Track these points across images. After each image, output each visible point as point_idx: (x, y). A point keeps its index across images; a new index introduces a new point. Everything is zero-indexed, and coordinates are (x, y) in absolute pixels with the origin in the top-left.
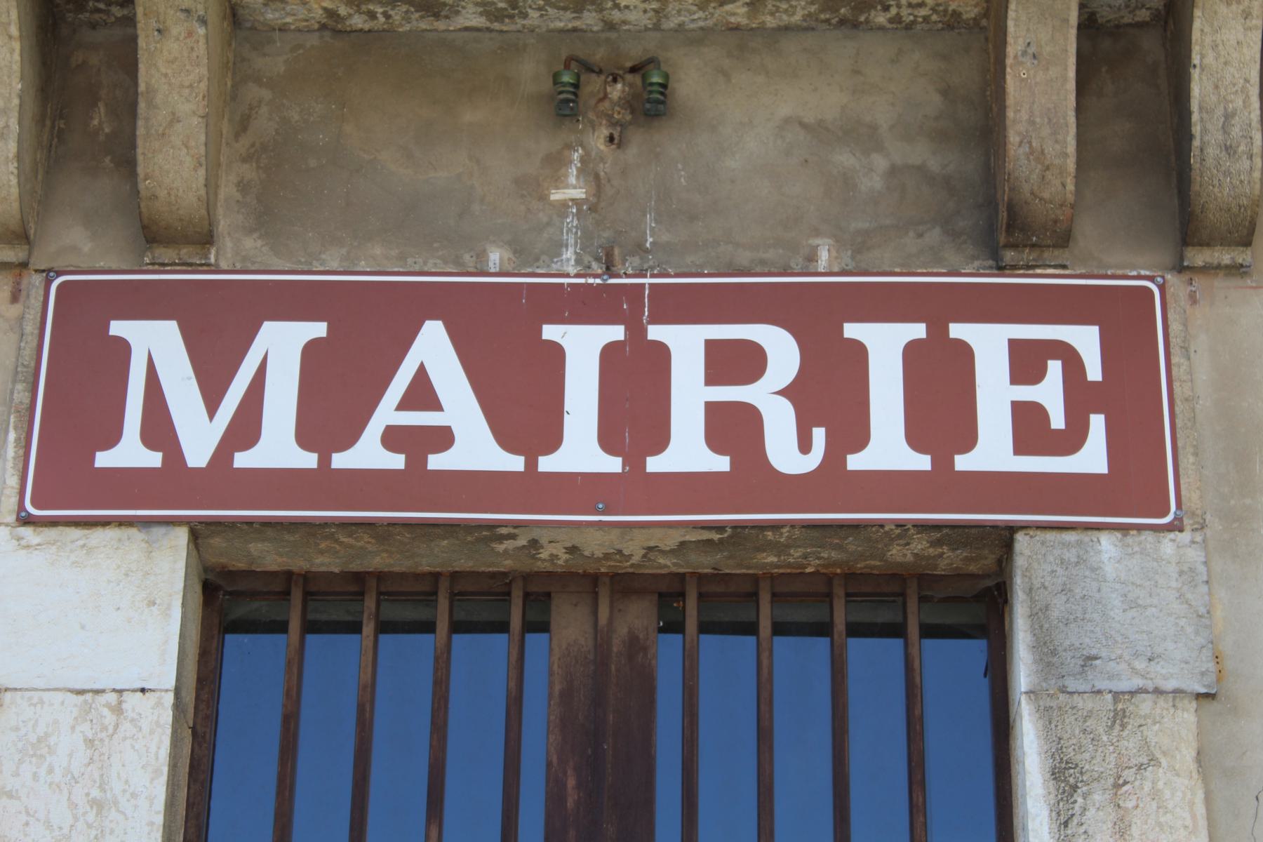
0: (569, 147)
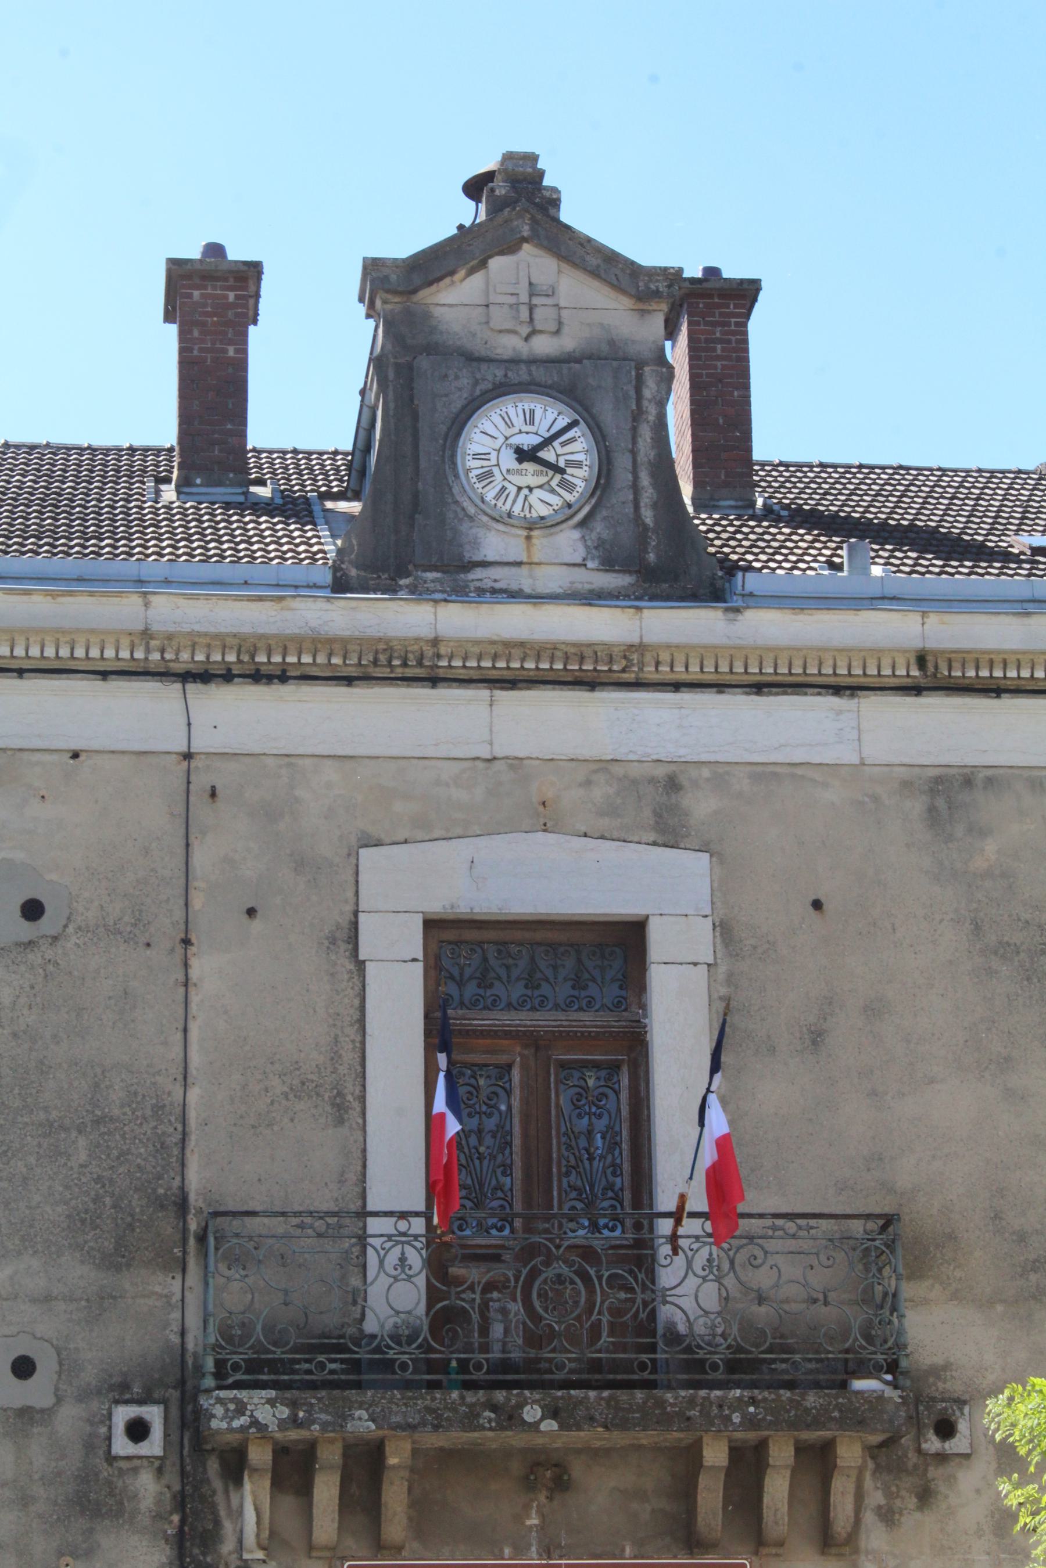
0: (532, 1500)
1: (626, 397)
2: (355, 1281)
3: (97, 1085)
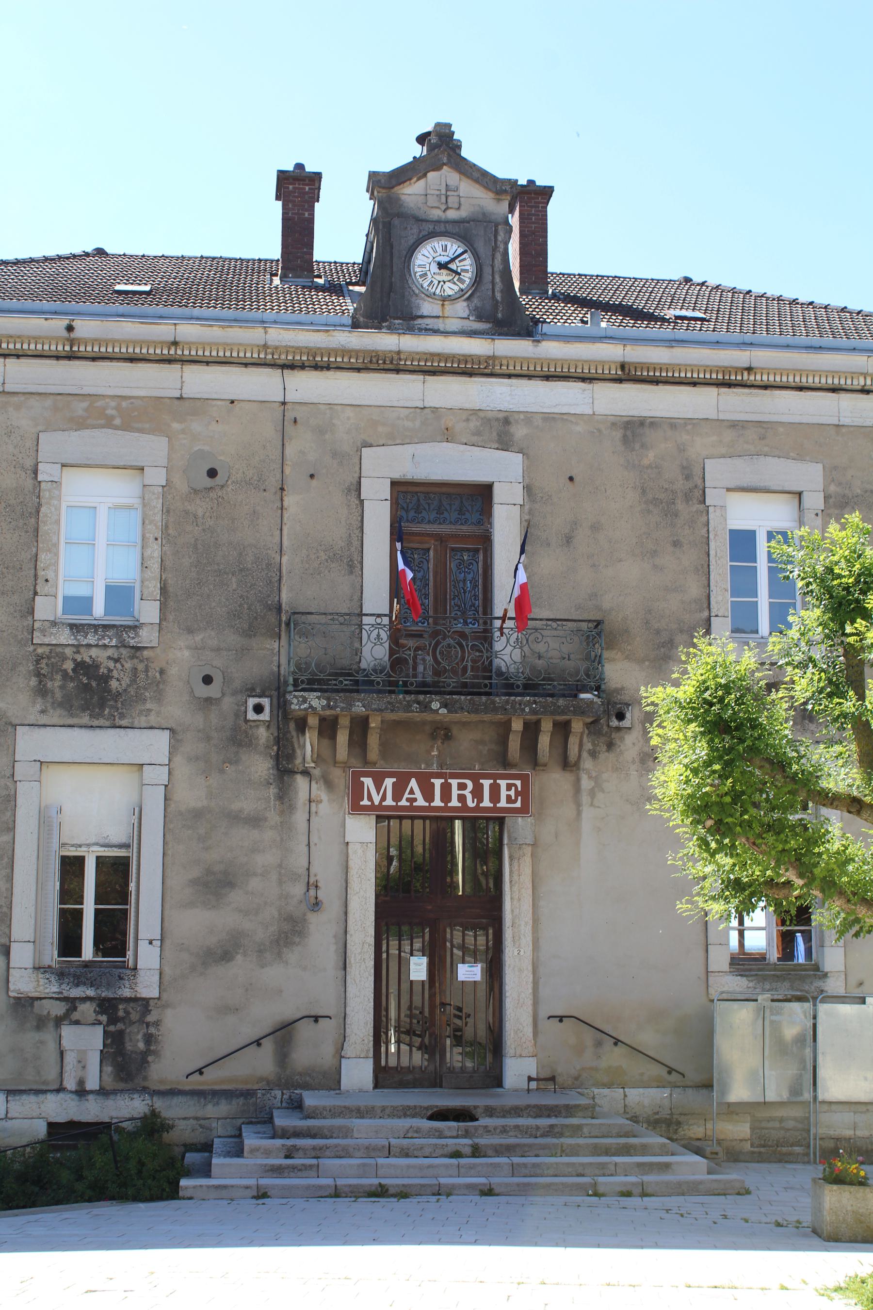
1: (490, 240)
2: (357, 645)
3: (241, 554)
